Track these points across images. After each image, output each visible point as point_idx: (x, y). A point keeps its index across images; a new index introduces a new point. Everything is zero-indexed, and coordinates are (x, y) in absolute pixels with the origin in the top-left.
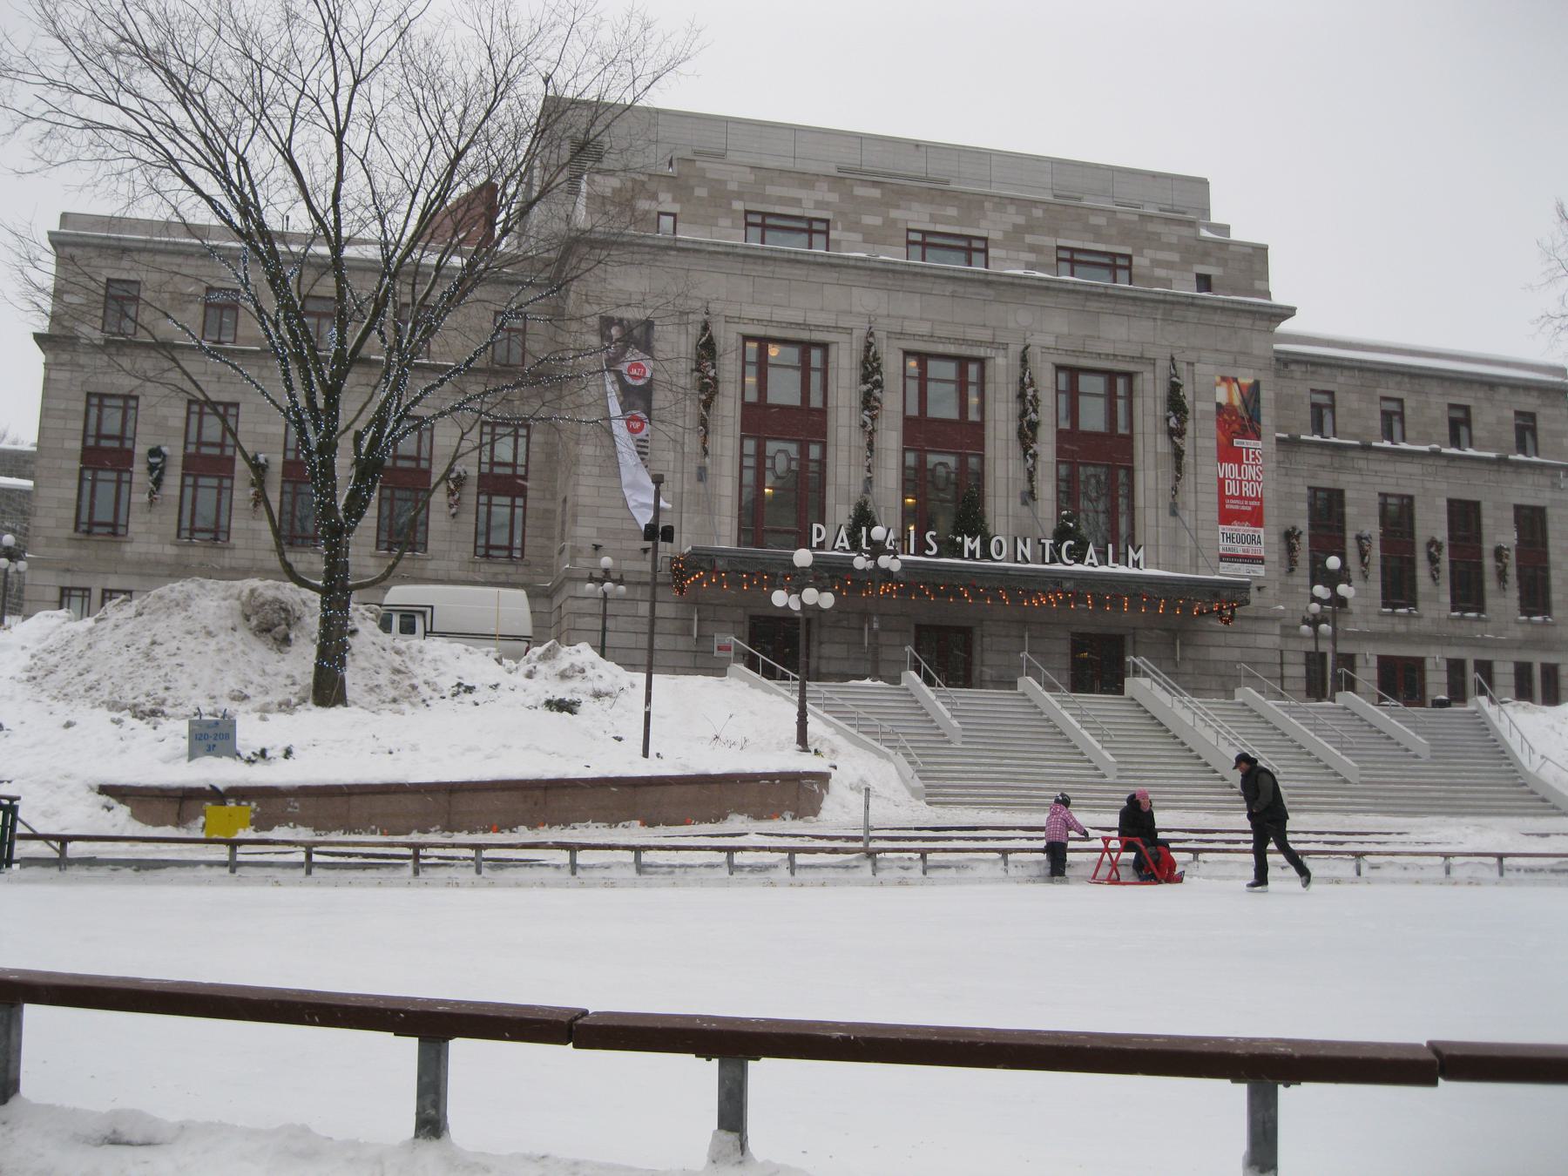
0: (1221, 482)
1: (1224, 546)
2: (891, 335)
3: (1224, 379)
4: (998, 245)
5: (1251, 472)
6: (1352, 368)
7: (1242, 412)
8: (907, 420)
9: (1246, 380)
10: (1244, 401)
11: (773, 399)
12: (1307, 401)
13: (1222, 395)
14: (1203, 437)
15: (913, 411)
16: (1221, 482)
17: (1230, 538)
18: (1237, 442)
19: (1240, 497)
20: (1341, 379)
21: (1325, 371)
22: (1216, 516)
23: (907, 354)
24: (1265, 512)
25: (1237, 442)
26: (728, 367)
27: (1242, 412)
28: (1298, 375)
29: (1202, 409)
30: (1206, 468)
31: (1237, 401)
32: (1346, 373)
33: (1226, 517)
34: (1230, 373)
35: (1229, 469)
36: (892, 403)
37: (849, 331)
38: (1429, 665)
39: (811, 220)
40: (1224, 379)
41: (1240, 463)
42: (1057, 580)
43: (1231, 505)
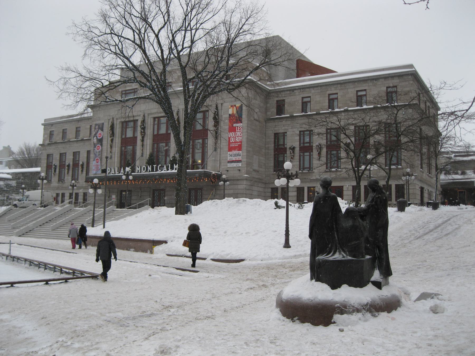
0: (229, 138)
1: (229, 158)
2: (148, 115)
3: (232, 106)
4: (175, 83)
5: (238, 134)
6: (317, 86)
7: (236, 115)
8: (154, 136)
9: (238, 105)
10: (237, 112)
11: (127, 136)
12: (301, 101)
13: (230, 112)
14: (224, 125)
15: (156, 133)
16: (229, 138)
17: (231, 156)
18: (234, 125)
19: (235, 142)
20: (313, 91)
21: (307, 90)
22: (227, 149)
23: (154, 118)
24: (242, 146)
25: (234, 125)
26: (118, 131)
27: (236, 115)
28: (297, 94)
29: (224, 117)
30: (225, 135)
31: (235, 112)
32: (315, 89)
33: (230, 149)
34: (233, 104)
35: (232, 134)
36: (149, 132)
37: (140, 115)
38: (344, 189)
39: (134, 89)
40: (232, 106)
41: (235, 131)
42: (153, 175)
43: (232, 145)
